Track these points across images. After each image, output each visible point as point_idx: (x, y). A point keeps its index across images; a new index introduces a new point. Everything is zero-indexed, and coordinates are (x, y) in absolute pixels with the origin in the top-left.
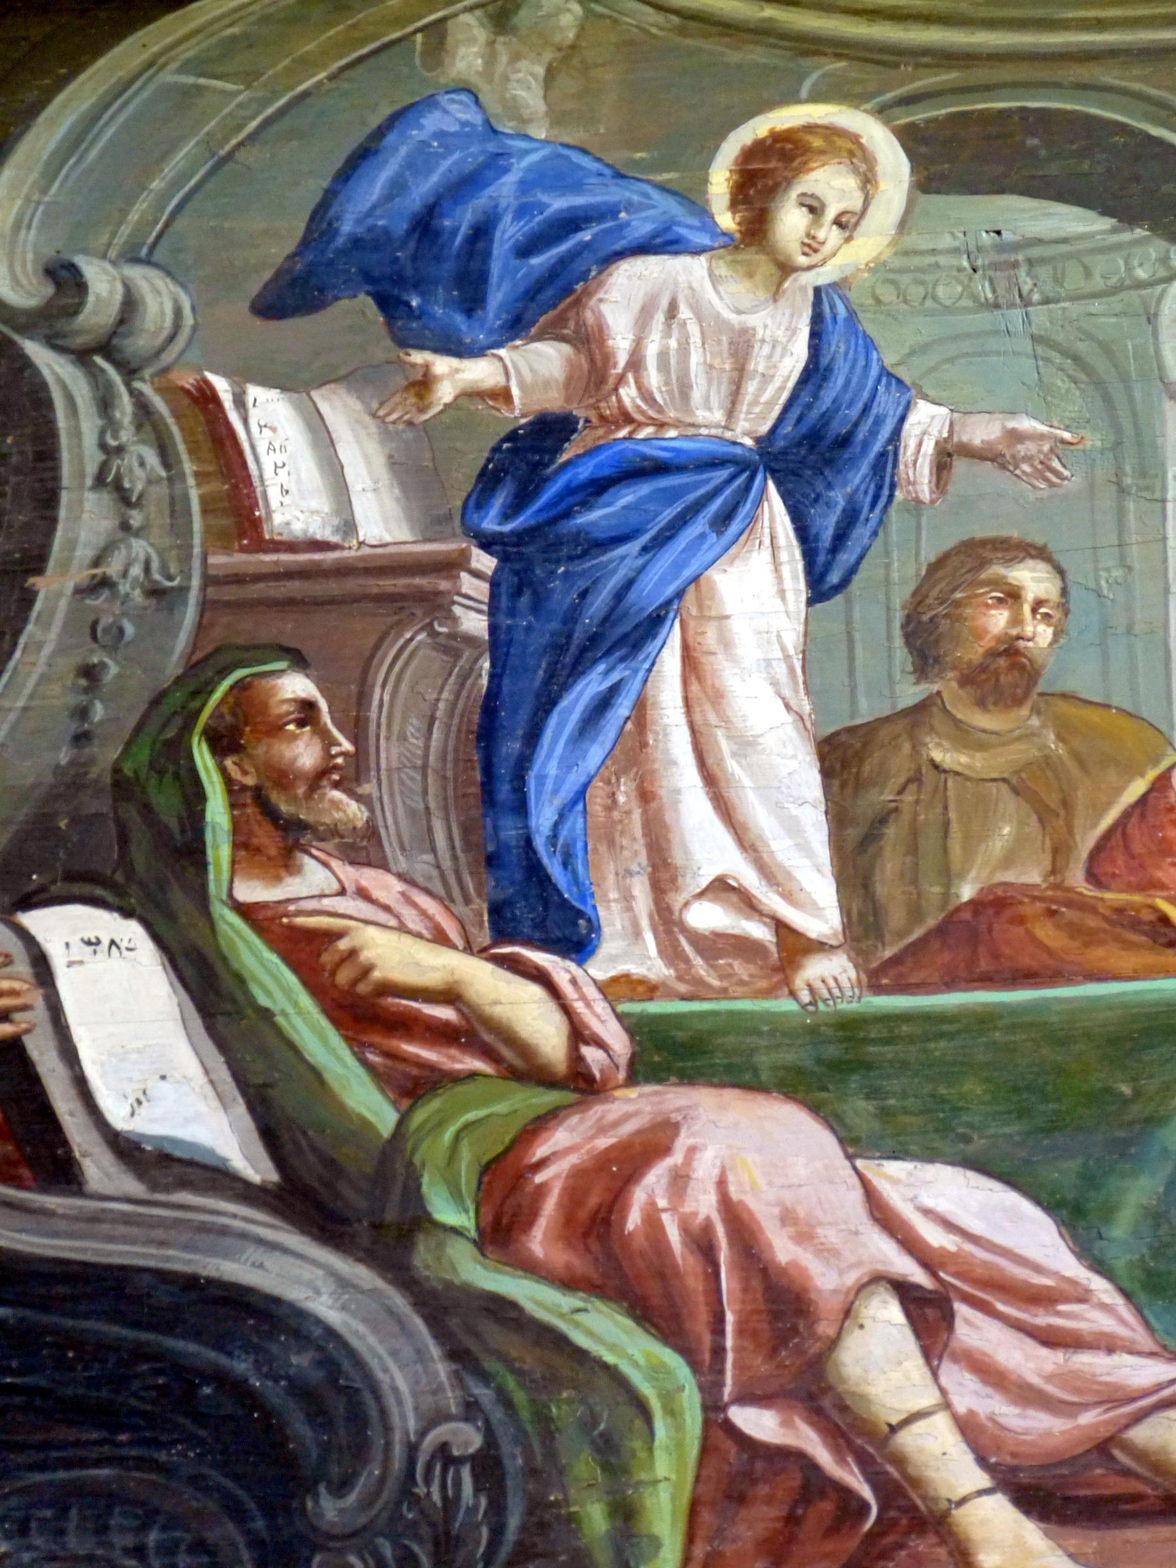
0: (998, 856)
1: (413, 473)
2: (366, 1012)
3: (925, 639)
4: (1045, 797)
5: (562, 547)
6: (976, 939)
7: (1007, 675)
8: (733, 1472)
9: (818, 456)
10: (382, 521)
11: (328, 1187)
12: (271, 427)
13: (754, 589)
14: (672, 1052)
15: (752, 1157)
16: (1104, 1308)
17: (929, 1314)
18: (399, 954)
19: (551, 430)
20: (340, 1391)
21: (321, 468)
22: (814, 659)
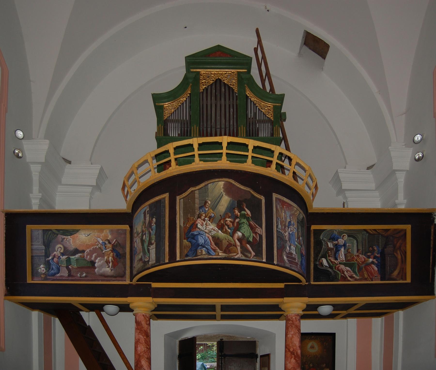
0: (349, 258)
1: (333, 245)
2: (332, 262)
3: (347, 251)
4: (350, 256)
5: (337, 248)
6: (348, 261)
7: (349, 252)
8: (342, 276)
9: (344, 245)
10: (332, 247)
11: (331, 267)
12: (329, 243)
13: (343, 249)
14: (340, 263)
15: (342, 267)
16: (352, 272)
17: (347, 272)
18: (333, 260)
19: (337, 244)
20: (331, 273)
21: (330, 245)
22: (344, 252)
